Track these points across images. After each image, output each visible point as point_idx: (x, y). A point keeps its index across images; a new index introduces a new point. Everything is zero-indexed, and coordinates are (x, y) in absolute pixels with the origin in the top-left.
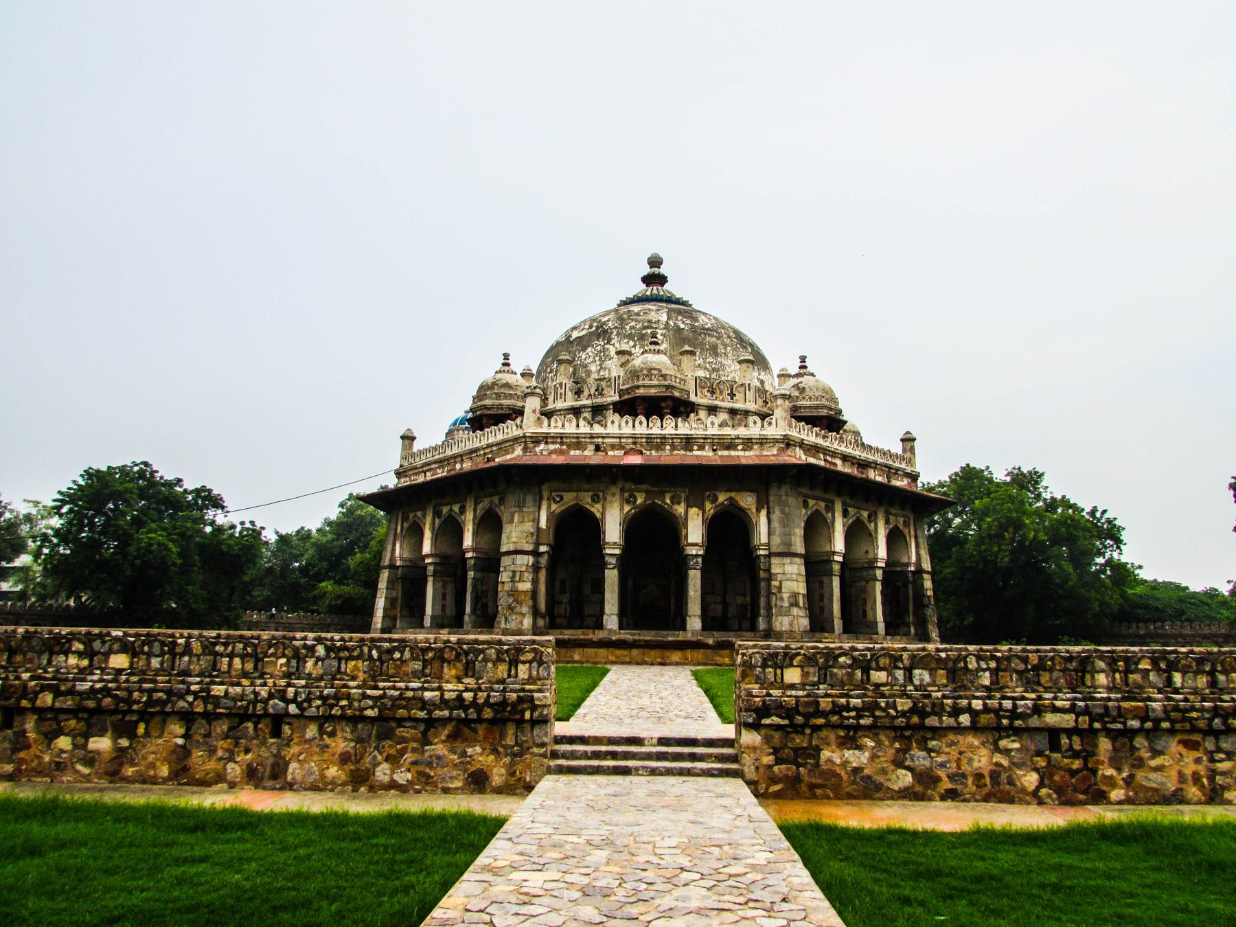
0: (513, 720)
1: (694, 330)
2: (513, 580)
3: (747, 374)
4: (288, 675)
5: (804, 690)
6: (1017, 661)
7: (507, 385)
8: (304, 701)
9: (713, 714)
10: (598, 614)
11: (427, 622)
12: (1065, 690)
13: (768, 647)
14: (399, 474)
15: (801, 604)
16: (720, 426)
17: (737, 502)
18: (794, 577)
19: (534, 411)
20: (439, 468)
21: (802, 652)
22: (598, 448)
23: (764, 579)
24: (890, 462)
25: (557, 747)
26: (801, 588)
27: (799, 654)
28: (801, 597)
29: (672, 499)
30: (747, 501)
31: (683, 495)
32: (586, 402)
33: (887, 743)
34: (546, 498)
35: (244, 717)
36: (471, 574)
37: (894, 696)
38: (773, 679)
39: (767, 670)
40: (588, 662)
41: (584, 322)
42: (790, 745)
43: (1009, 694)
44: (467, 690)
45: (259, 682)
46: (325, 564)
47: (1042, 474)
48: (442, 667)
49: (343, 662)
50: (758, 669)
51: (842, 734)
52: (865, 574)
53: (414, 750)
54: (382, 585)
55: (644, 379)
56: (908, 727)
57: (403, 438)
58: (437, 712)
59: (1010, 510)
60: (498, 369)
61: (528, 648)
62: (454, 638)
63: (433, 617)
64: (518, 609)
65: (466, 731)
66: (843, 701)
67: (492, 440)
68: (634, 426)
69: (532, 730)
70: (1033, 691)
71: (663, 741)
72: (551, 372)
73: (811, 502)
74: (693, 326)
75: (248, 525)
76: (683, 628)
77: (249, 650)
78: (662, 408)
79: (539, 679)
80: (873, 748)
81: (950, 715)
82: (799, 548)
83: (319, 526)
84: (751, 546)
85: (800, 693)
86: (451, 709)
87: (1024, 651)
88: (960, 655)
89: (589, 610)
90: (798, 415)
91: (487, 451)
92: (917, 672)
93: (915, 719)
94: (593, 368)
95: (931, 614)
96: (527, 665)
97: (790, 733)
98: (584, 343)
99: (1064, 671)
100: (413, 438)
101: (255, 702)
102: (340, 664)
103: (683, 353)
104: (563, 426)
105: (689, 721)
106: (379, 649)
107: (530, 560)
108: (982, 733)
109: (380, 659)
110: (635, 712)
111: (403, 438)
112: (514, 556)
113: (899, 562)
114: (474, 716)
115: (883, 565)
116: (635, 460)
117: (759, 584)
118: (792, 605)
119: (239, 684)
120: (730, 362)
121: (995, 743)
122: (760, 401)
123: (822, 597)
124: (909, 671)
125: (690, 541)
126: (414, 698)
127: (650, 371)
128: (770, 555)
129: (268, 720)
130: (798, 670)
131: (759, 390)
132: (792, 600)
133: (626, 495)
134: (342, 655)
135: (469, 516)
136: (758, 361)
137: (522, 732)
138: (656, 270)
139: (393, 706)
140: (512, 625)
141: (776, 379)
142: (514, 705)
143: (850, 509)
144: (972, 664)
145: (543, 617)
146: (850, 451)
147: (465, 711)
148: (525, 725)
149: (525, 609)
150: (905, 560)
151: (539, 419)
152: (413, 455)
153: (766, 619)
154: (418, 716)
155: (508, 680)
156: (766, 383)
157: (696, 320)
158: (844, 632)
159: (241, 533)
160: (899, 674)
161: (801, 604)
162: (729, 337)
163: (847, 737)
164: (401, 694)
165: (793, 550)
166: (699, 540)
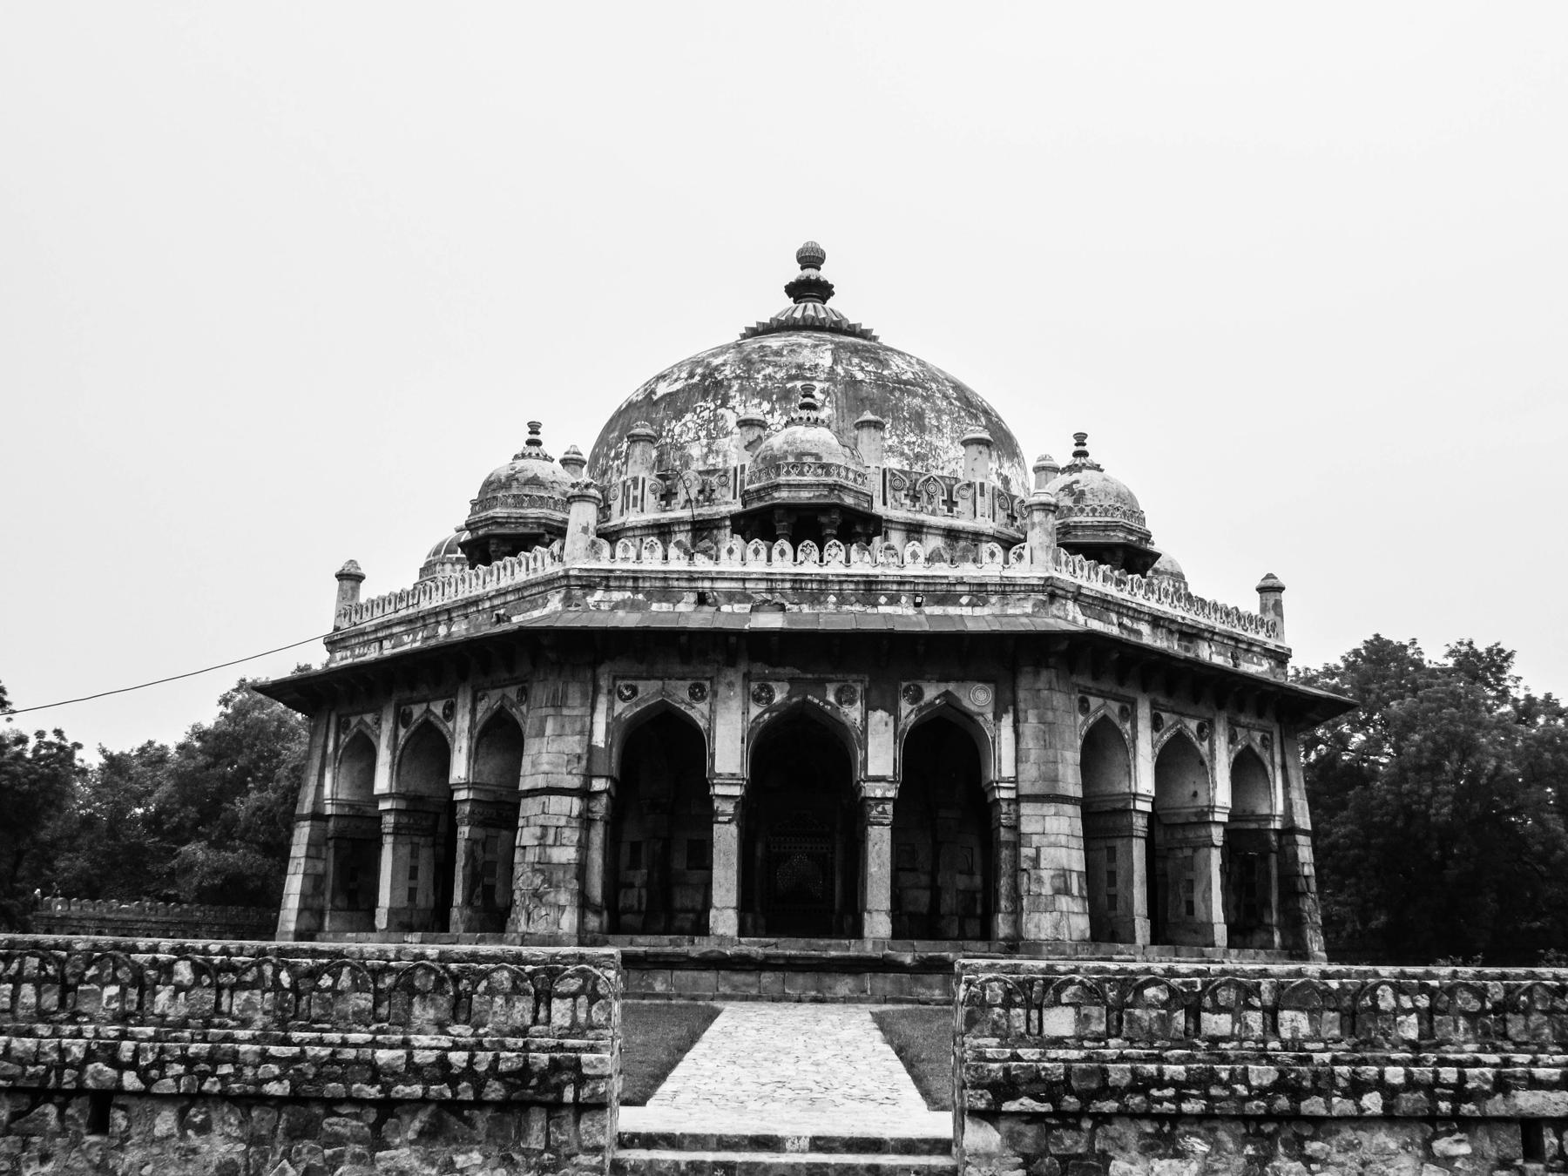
0: (541, 1104)
1: (880, 382)
2: (542, 845)
3: (977, 465)
4: (122, 1018)
5: (1081, 1047)
6: (1466, 995)
7: (535, 481)
8: (152, 1066)
9: (911, 1093)
10: (699, 907)
11: (381, 920)
12: (1552, 1049)
13: (1015, 969)
14: (332, 644)
15: (1075, 891)
16: (928, 560)
17: (958, 700)
18: (1063, 840)
19: (585, 530)
20: (407, 633)
21: (1078, 978)
22: (702, 599)
23: (1007, 843)
24: (1238, 630)
25: (623, 1154)
27: (1071, 982)
28: (1074, 876)
29: (838, 695)
30: (978, 699)
31: (859, 688)
32: (679, 513)
33: (1231, 1146)
34: (605, 691)
35: (40, 1094)
36: (464, 831)
37: (1244, 1059)
38: (1023, 1030)
39: (1013, 1012)
40: (679, 996)
41: (680, 366)
42: (1053, 1150)
43: (1451, 1056)
44: (456, 1047)
45: (68, 1029)
46: (192, 811)
47: (1510, 655)
48: (410, 1004)
49: (226, 993)
50: (997, 1010)
51: (1149, 1130)
52: (1191, 835)
53: (358, 1159)
54: (299, 850)
55: (788, 473)
56: (1269, 1116)
57: (341, 576)
58: (400, 1087)
59: (1452, 720)
60: (519, 451)
61: (571, 969)
62: (432, 951)
63: (392, 912)
64: (551, 897)
65: (453, 1119)
66: (1151, 1068)
67: (506, 582)
68: (769, 559)
69: (577, 1122)
70: (1496, 1050)
71: (820, 1144)
72: (617, 457)
73: (1094, 702)
74: (880, 377)
75: (50, 737)
76: (857, 932)
77: (50, 969)
78: (822, 526)
79: (592, 1028)
80: (1206, 1155)
81: (1346, 1095)
82: (1075, 790)
83: (182, 739)
84: (984, 783)
85: (1074, 1054)
86: (427, 1083)
87: (1479, 976)
88: (1364, 985)
89: (682, 899)
90: (1071, 543)
91: (496, 602)
92: (1285, 1015)
93: (1283, 1103)
94: (695, 451)
95: (1310, 907)
96: (569, 1001)
97: (1056, 1127)
98: (677, 404)
99: (1550, 1012)
100: (359, 578)
101: (61, 1066)
102: (219, 996)
103: (861, 425)
104: (638, 558)
105: (869, 1106)
106: (292, 968)
108: (1403, 1127)
109: (294, 987)
110: (768, 1089)
111: (341, 576)
112: (544, 798)
113: (1253, 814)
114: (469, 1096)
115: (1225, 819)
116: (771, 621)
117: (998, 855)
118: (1057, 892)
119: (30, 1033)
120: (947, 442)
121: (1427, 1146)
122: (1001, 516)
123: (1112, 875)
124: (1271, 1013)
125: (871, 772)
126: (357, 1061)
127: (800, 459)
128: (1018, 800)
129: (83, 1101)
130: (1071, 1011)
131: (1001, 495)
132: (1059, 883)
133: (754, 686)
134: (223, 979)
135: (462, 722)
136: (999, 442)
137: (559, 1126)
138: (811, 273)
139: (315, 1075)
140: (540, 928)
141: (1032, 476)
142: (544, 1075)
143: (1164, 715)
144: (1387, 1001)
145: (598, 912)
146: (1166, 608)
147: (453, 1081)
148: (564, 1113)
149: (564, 898)
150: (1265, 810)
151: (593, 543)
152: (359, 609)
153: (1010, 918)
154: (364, 1095)
155: (533, 1030)
156: (1013, 483)
157: (884, 364)
158: (1154, 942)
159: (36, 751)
160: (1255, 1019)
161: (1075, 891)
162: (946, 397)
163: (1158, 1134)
164: (333, 1054)
165: (1061, 792)
166: (891, 773)
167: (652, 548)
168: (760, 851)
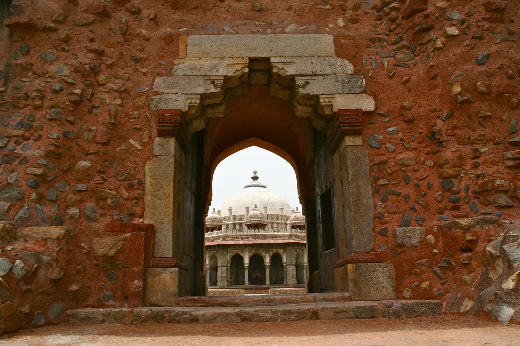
7: (215, 218)
22: (242, 238)
26: (295, 273)
29: (261, 251)
30: (281, 251)
36: (208, 271)
73: (298, 250)
76: (265, 284)
78: (258, 227)
107: (226, 268)
122: (286, 219)
123: (301, 274)
125: (266, 262)
127: (255, 216)
138: (255, 175)
149: (225, 281)
167: (234, 231)
168: (251, 272)
